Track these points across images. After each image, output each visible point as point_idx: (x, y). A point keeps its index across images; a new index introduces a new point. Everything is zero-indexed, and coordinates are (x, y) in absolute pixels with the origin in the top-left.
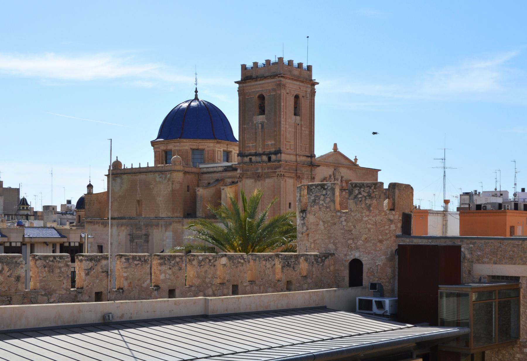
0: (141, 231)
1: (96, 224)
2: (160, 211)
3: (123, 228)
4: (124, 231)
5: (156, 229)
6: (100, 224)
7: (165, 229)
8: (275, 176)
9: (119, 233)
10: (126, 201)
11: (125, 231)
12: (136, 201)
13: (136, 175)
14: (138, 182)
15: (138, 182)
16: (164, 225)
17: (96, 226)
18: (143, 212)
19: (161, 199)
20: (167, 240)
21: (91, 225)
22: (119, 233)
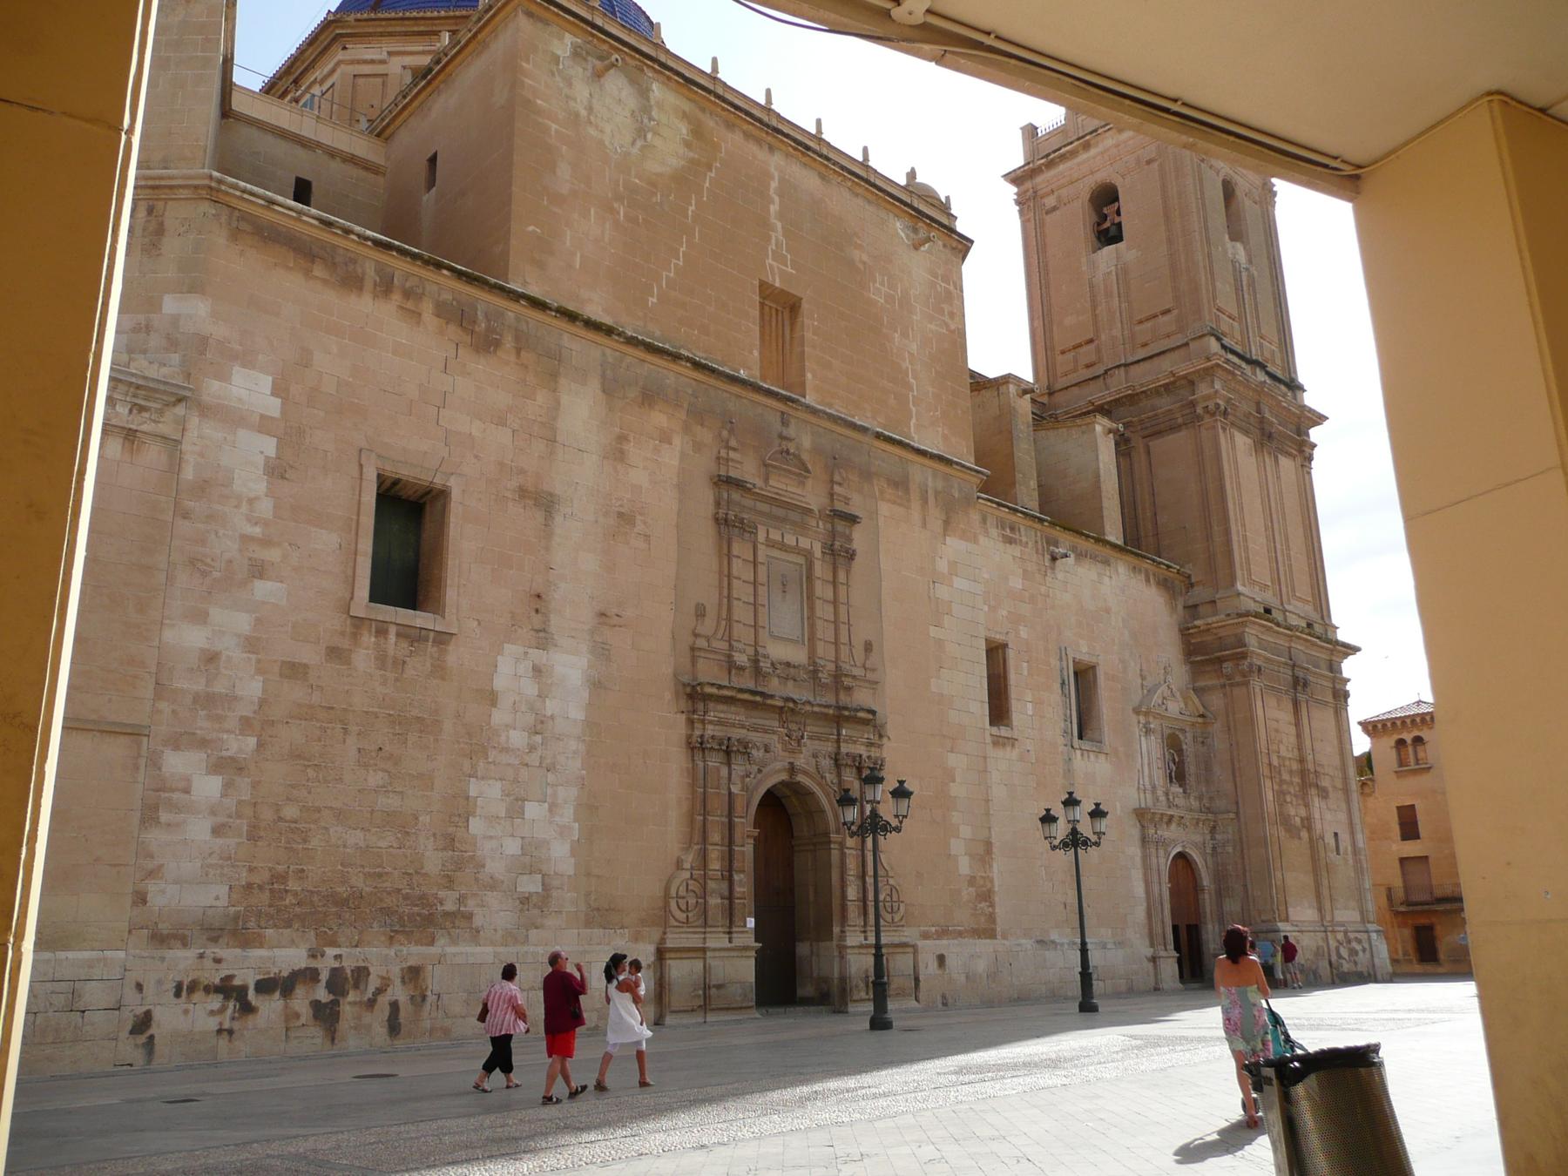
0: (802, 484)
1: (369, 284)
2: (914, 409)
3: (659, 418)
4: (665, 438)
5: (894, 503)
6: (427, 308)
7: (944, 518)
8: (1294, 457)
9: (622, 438)
10: (683, 249)
11: (677, 441)
12: (757, 283)
13: (759, 141)
14: (774, 185)
15: (774, 185)
16: (937, 493)
17: (365, 304)
18: (809, 376)
19: (914, 347)
20: (959, 583)
21: (307, 273)
22: (622, 438)
